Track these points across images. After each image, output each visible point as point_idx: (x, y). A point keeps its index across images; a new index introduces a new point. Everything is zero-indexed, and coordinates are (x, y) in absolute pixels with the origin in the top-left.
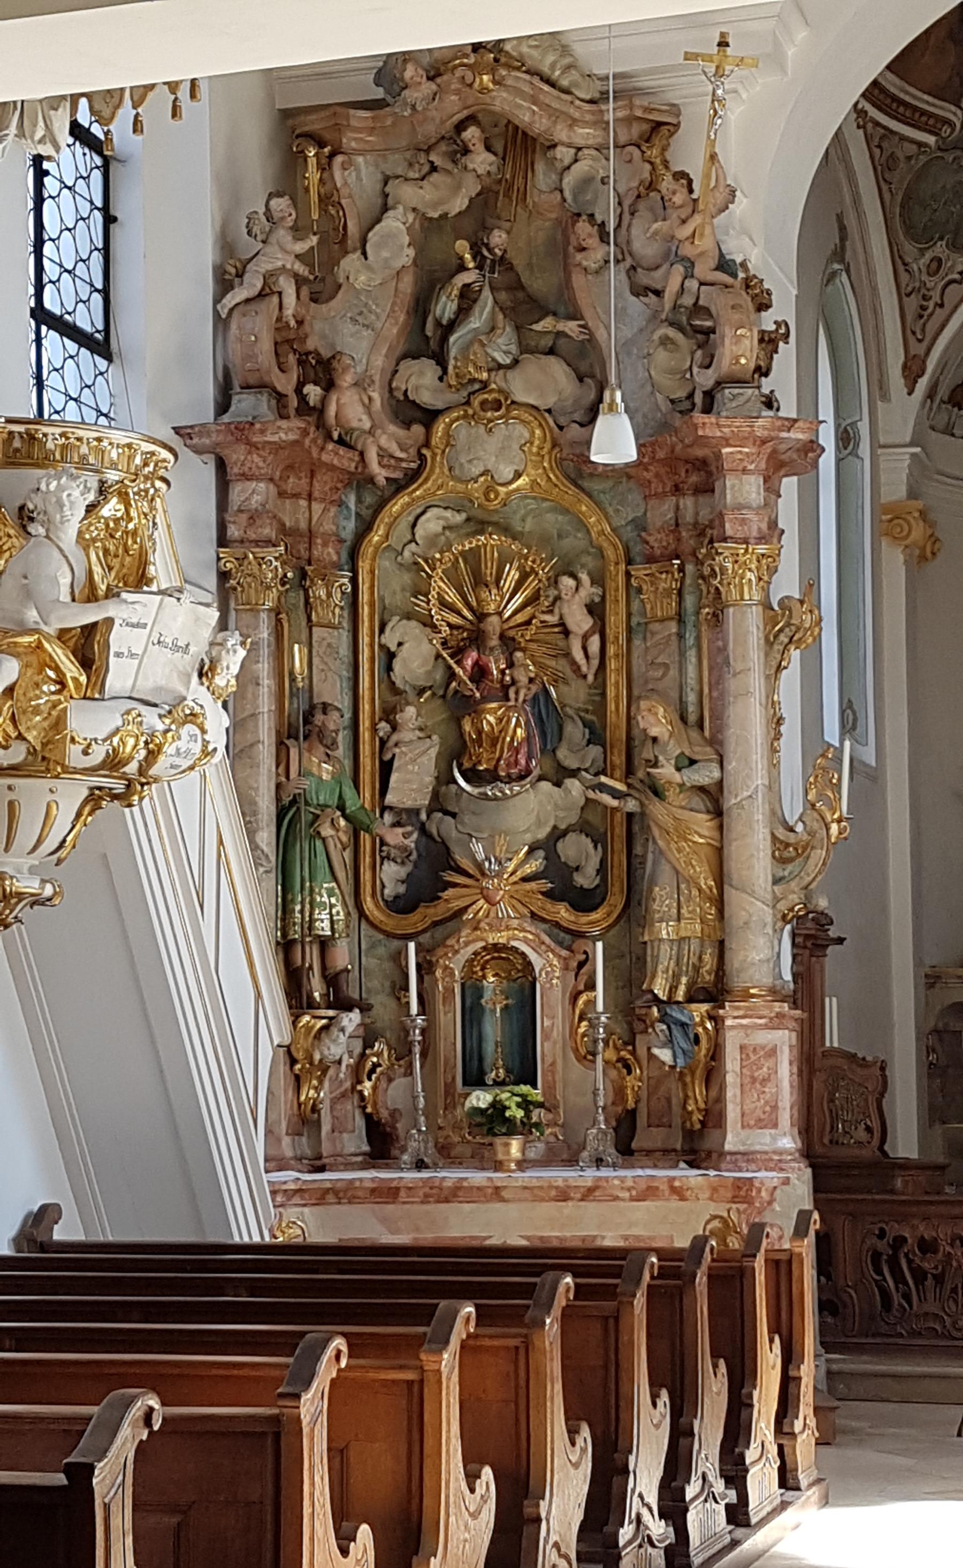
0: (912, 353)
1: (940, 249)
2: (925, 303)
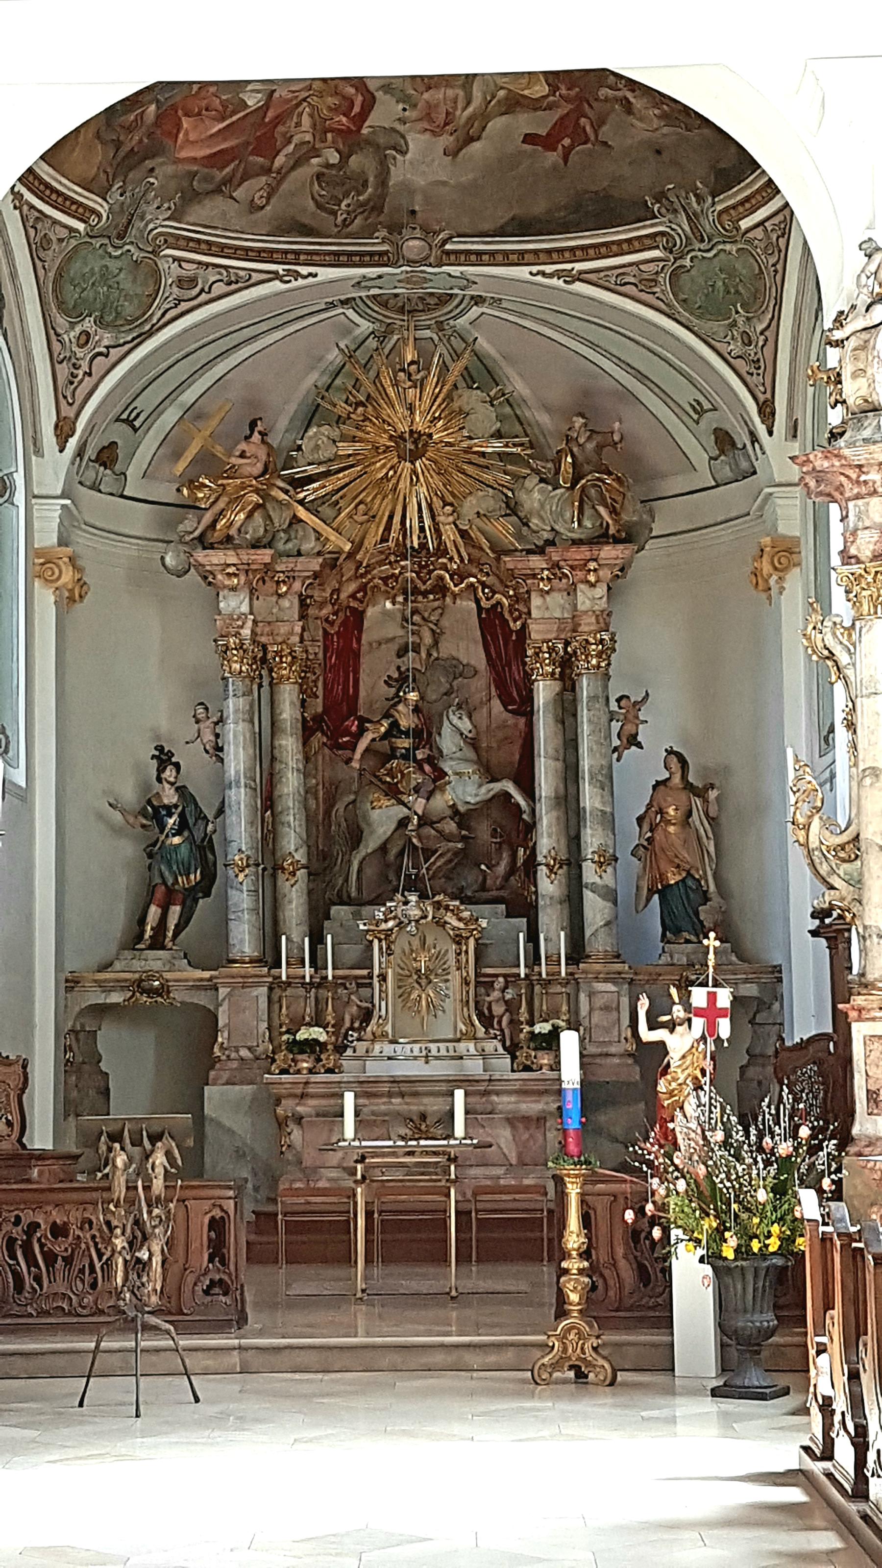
0: (63, 414)
1: (88, 324)
2: (75, 371)
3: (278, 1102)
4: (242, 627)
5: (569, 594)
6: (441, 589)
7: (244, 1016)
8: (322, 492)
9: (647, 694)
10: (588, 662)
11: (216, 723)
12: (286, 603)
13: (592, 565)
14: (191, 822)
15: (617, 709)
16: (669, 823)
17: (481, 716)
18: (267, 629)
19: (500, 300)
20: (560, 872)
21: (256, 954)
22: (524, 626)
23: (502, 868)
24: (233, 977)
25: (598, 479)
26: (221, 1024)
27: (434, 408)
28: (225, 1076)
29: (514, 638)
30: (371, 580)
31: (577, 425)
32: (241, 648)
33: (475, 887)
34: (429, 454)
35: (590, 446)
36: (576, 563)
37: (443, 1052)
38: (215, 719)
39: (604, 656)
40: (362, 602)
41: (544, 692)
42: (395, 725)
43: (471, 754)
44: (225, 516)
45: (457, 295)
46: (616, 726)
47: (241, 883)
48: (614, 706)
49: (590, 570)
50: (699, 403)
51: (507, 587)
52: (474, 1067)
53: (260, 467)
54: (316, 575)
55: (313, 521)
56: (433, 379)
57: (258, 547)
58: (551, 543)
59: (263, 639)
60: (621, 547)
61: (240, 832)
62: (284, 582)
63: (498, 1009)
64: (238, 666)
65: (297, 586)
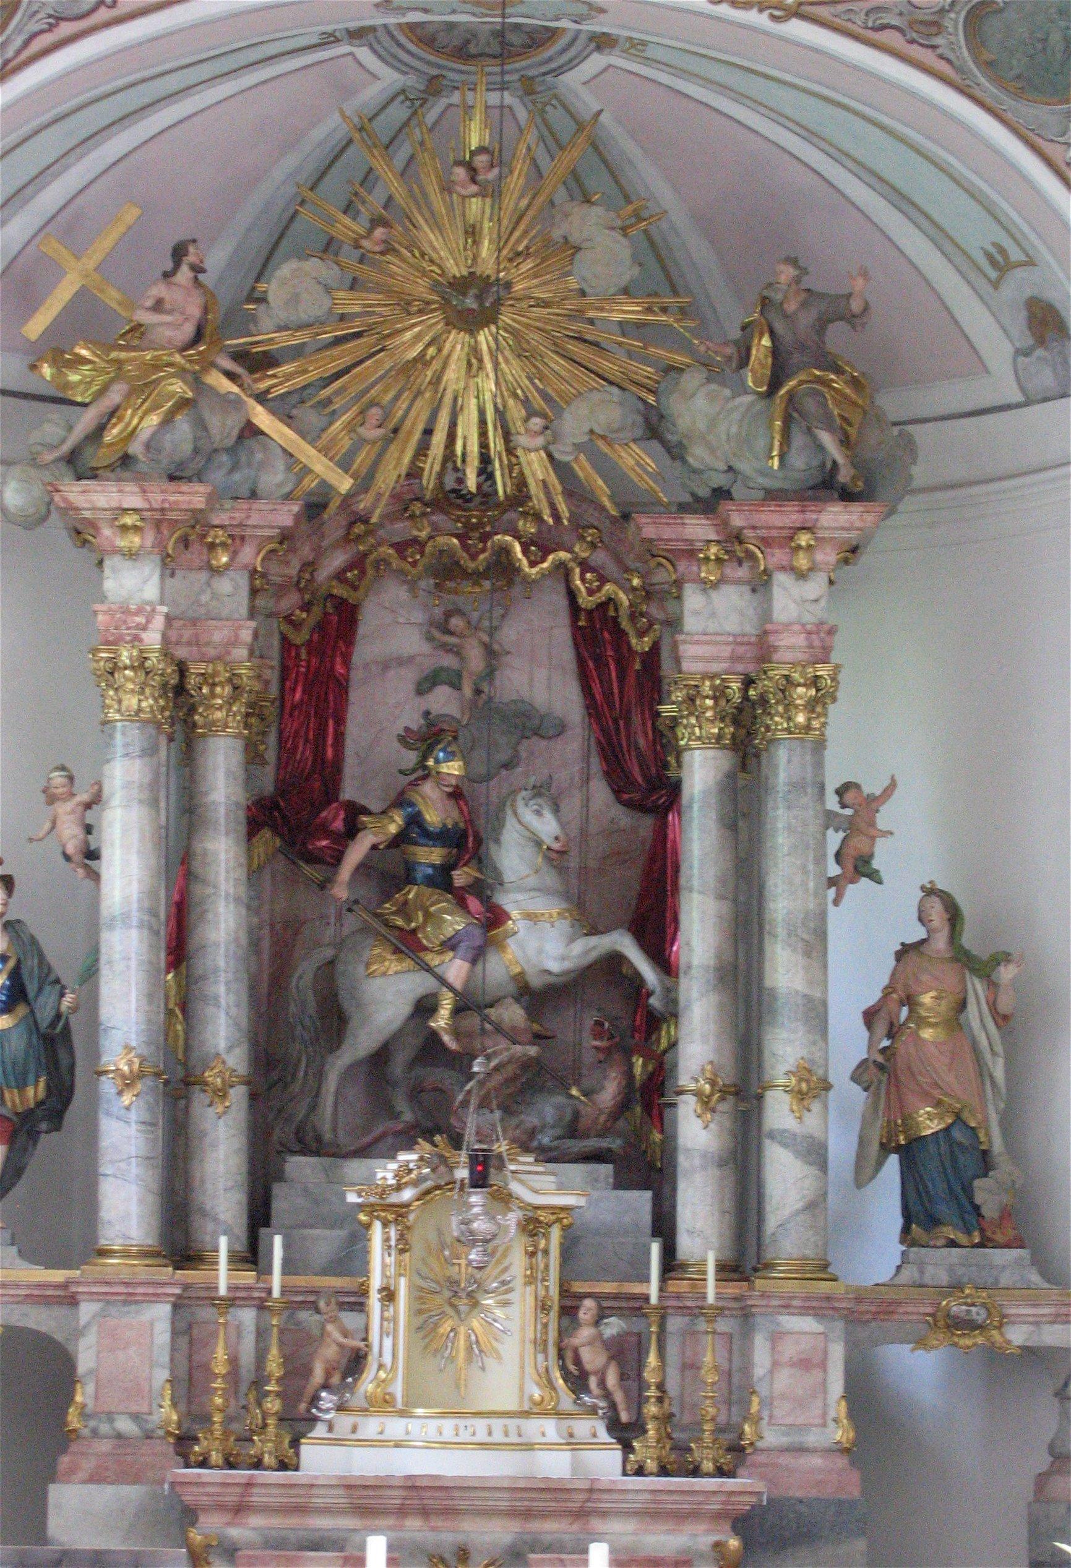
3: (189, 1515)
4: (144, 628)
5: (754, 591)
6: (503, 568)
7: (124, 1354)
8: (299, 381)
9: (892, 786)
10: (789, 719)
11: (88, 806)
12: (224, 585)
13: (804, 539)
14: (31, 988)
15: (836, 808)
16: (922, 1022)
17: (572, 805)
18: (187, 634)
19: (644, 43)
20: (723, 1107)
21: (150, 1242)
22: (656, 647)
23: (609, 1092)
24: (107, 1283)
25: (819, 380)
26: (81, 1369)
27: (517, 234)
28: (88, 1465)
29: (637, 666)
30: (374, 547)
31: (783, 279)
32: (142, 665)
33: (558, 1131)
34: (505, 318)
35: (806, 320)
36: (775, 533)
37: (498, 1437)
38: (85, 797)
39: (819, 709)
40: (355, 588)
41: (701, 771)
42: (415, 821)
43: (551, 879)
44: (120, 420)
45: (564, 30)
46: (834, 839)
47: (128, 1108)
48: (832, 802)
49: (799, 547)
50: (1002, 250)
51: (627, 570)
52: (555, 1465)
53: (189, 329)
54: (286, 537)
55: (283, 434)
56: (516, 181)
57: (180, 478)
58: (722, 493)
59: (181, 653)
60: (856, 508)
61: (124, 1011)
62: (224, 545)
63: (593, 1358)
64: (134, 702)
65: (248, 554)
